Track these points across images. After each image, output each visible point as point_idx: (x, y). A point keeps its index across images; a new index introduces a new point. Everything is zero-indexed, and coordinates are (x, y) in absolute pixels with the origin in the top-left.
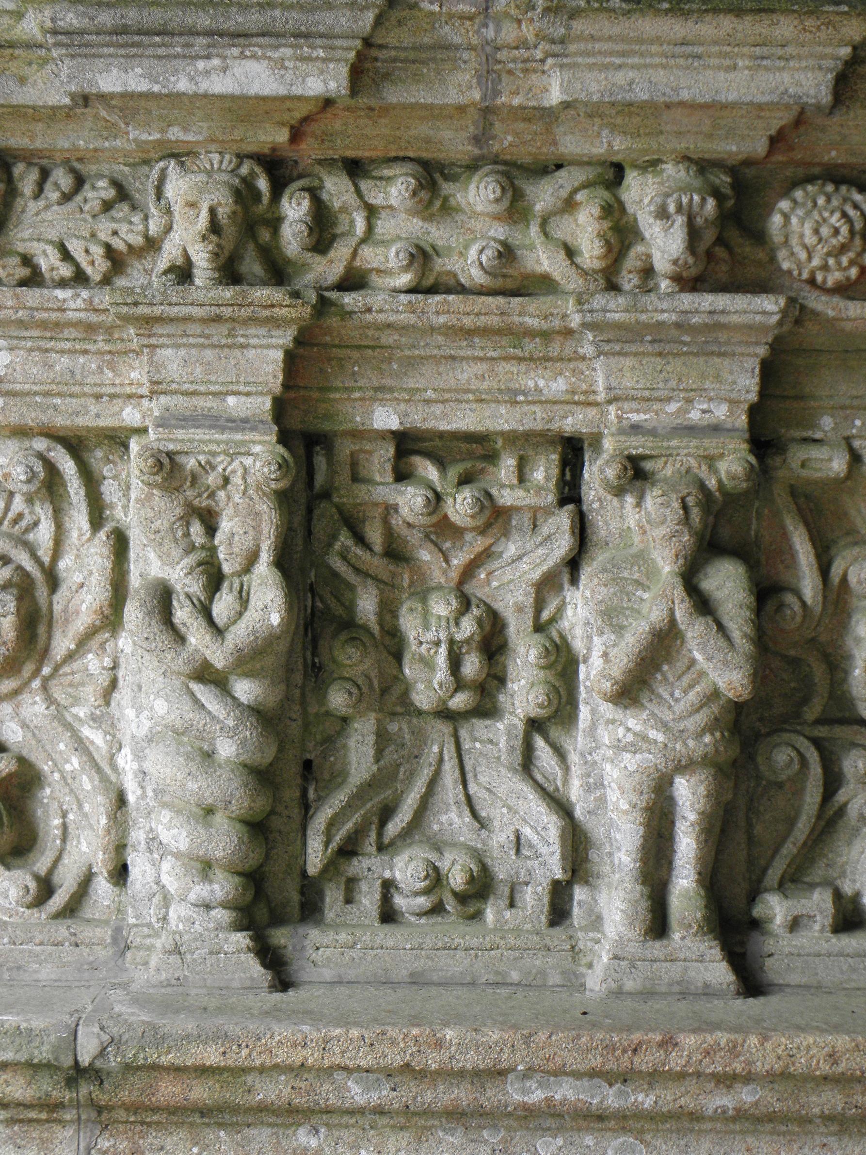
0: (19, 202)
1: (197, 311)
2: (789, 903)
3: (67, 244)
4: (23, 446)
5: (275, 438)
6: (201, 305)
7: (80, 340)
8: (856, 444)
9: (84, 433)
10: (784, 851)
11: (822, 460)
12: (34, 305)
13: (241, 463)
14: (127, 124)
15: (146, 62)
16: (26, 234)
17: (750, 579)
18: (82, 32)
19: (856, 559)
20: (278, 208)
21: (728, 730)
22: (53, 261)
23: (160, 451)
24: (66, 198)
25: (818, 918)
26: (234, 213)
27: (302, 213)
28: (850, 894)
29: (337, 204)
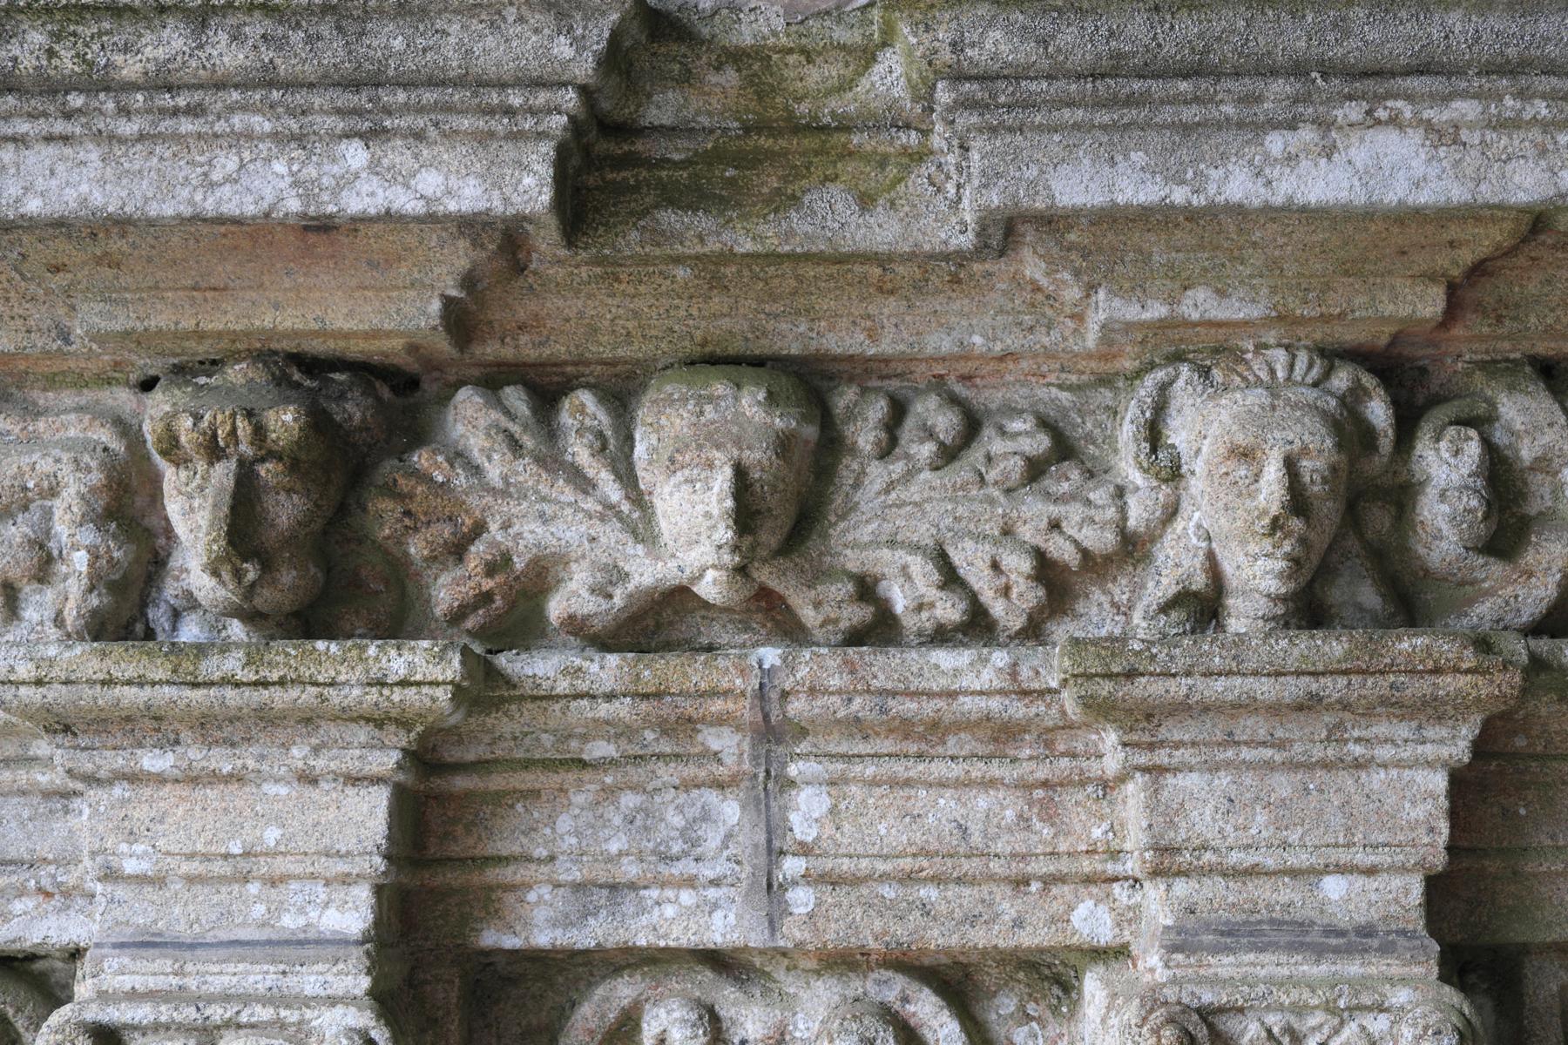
0: (848, 468)
1: (1265, 688)
3: (951, 552)
4: (850, 993)
5: (1436, 970)
6: (1278, 674)
7: (981, 758)
9: (974, 958)
12: (889, 686)
13: (1363, 1028)
14: (1091, 288)
15: (1153, 138)
16: (865, 533)
18: (1018, 74)
20: (1406, 462)
22: (923, 590)
23: (1186, 1009)
24: (949, 455)
26: (1334, 469)
27: (1465, 471)
29: (1527, 453)
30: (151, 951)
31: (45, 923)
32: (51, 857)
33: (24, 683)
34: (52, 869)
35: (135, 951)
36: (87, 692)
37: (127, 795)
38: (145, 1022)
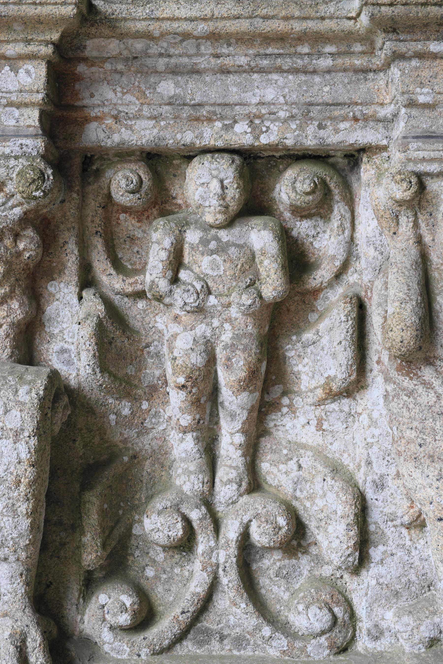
30: (432, 140)
31: (356, 134)
32: (359, 101)
33: (384, 5)
34: (360, 107)
35: (424, 140)
36: (414, 9)
37: (418, 65)
38: (435, 171)
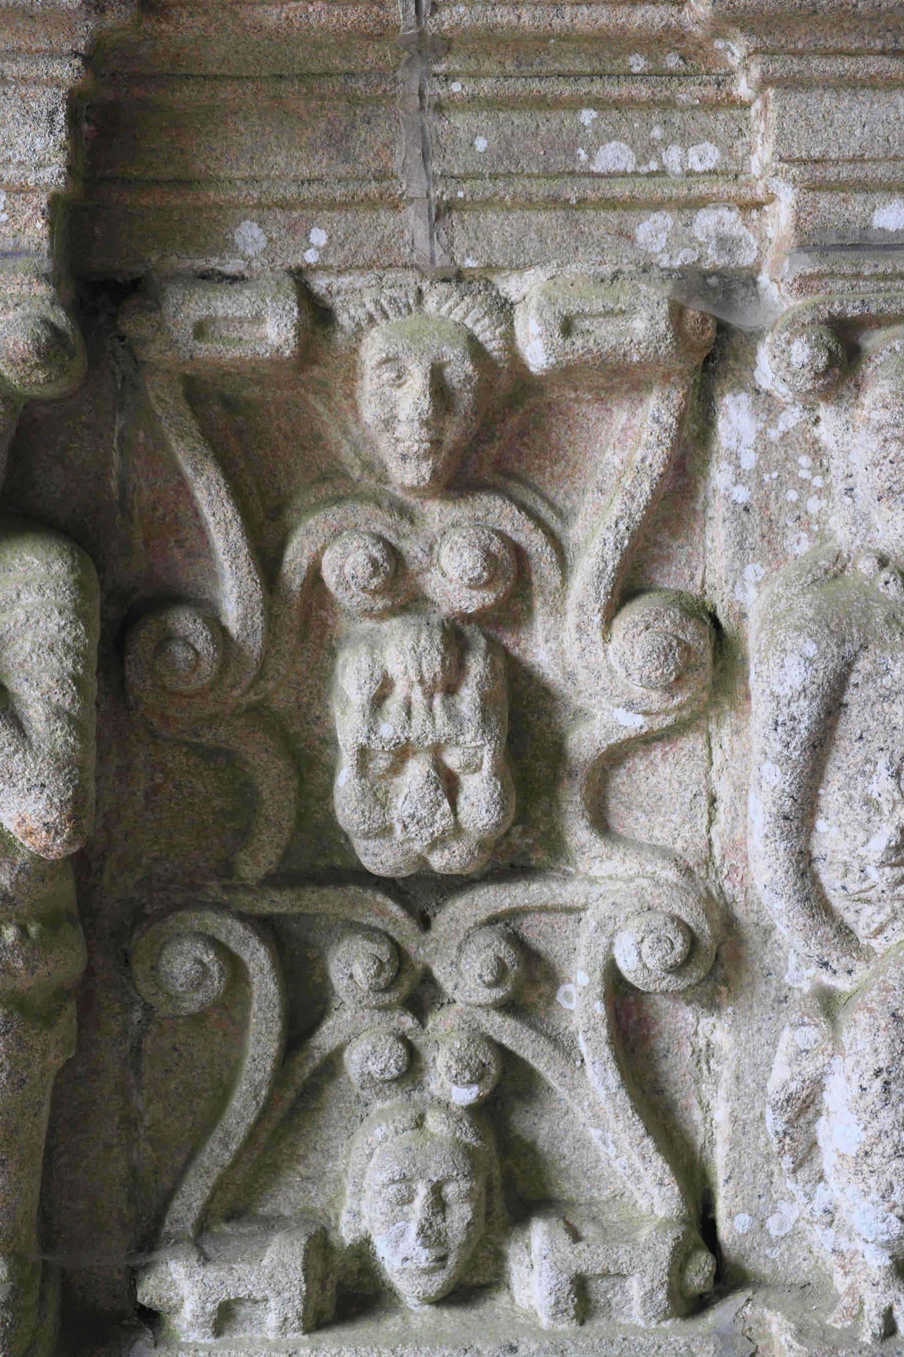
2: (212, 1273)
8: (320, 284)
10: (204, 1159)
11: (241, 321)
17: (80, 586)
19: (336, 534)
21: (40, 918)
25: (272, 1304)
28: (348, 1241)
